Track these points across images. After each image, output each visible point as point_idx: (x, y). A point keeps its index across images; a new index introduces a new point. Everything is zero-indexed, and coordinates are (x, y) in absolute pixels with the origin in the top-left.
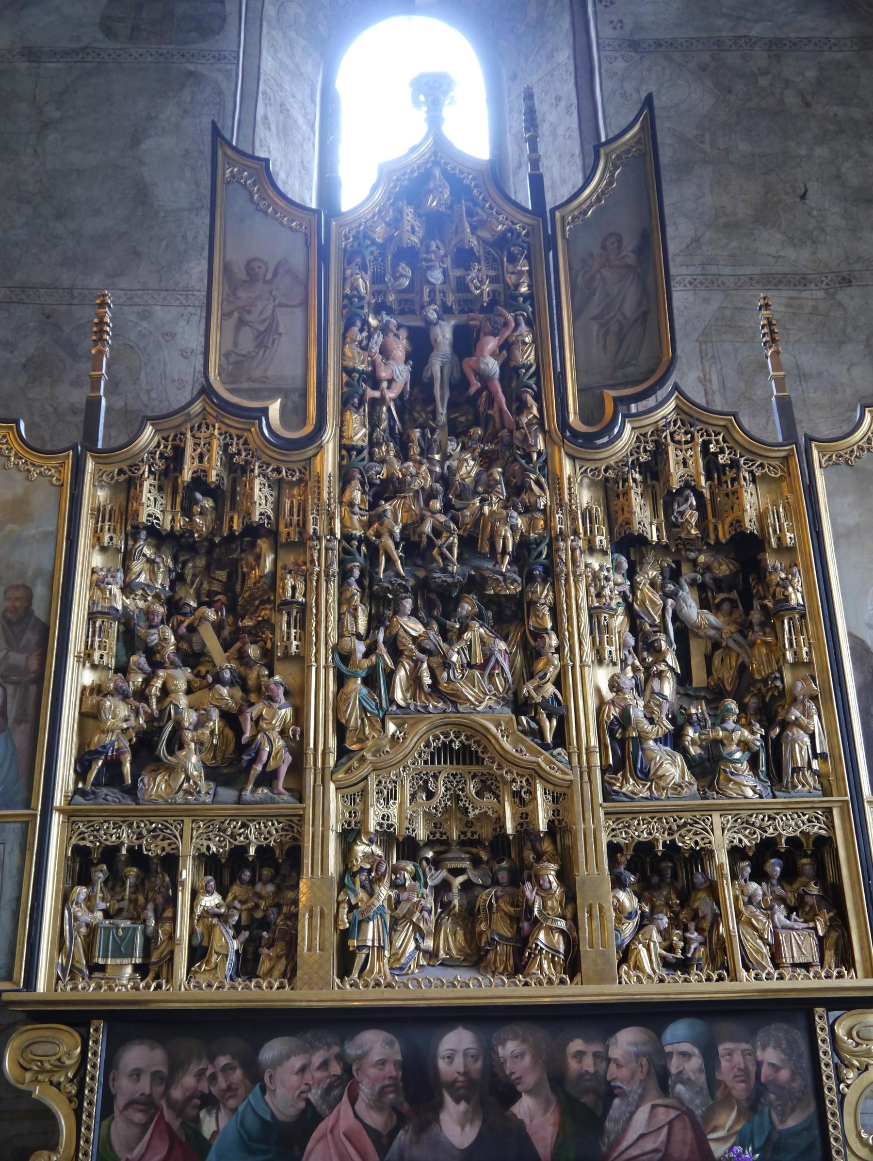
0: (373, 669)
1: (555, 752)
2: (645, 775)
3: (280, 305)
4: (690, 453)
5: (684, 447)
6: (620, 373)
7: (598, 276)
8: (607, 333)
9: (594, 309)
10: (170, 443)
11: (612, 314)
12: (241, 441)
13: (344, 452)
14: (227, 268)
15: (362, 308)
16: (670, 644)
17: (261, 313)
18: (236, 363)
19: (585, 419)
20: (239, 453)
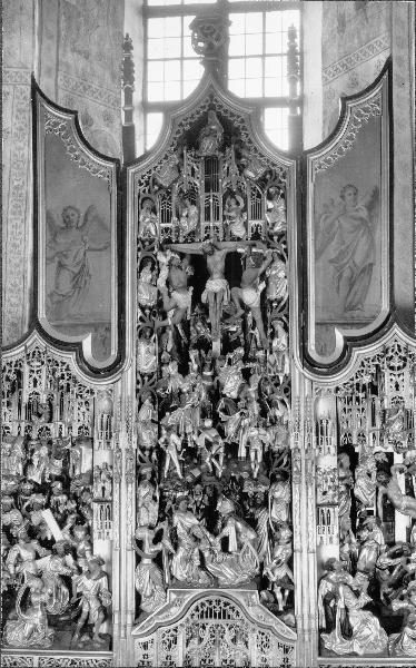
0: (160, 554)
1: (285, 618)
2: (347, 633)
3: (90, 249)
4: (401, 378)
5: (396, 373)
6: (348, 314)
7: (337, 222)
8: (341, 276)
9: (332, 252)
10: (13, 369)
11: (345, 261)
12: (64, 367)
13: (139, 378)
14: (49, 217)
15: (153, 249)
16: (378, 523)
17: (75, 257)
18: (59, 302)
19: (321, 352)
20: (63, 377)
